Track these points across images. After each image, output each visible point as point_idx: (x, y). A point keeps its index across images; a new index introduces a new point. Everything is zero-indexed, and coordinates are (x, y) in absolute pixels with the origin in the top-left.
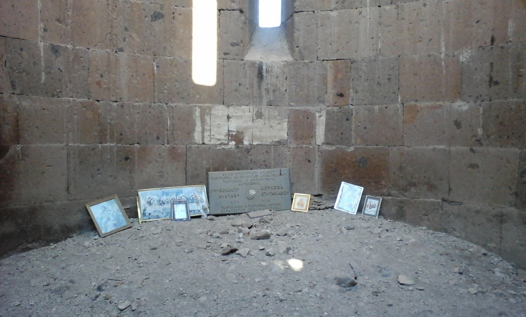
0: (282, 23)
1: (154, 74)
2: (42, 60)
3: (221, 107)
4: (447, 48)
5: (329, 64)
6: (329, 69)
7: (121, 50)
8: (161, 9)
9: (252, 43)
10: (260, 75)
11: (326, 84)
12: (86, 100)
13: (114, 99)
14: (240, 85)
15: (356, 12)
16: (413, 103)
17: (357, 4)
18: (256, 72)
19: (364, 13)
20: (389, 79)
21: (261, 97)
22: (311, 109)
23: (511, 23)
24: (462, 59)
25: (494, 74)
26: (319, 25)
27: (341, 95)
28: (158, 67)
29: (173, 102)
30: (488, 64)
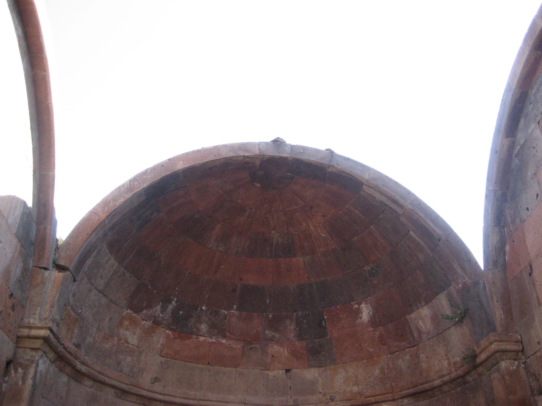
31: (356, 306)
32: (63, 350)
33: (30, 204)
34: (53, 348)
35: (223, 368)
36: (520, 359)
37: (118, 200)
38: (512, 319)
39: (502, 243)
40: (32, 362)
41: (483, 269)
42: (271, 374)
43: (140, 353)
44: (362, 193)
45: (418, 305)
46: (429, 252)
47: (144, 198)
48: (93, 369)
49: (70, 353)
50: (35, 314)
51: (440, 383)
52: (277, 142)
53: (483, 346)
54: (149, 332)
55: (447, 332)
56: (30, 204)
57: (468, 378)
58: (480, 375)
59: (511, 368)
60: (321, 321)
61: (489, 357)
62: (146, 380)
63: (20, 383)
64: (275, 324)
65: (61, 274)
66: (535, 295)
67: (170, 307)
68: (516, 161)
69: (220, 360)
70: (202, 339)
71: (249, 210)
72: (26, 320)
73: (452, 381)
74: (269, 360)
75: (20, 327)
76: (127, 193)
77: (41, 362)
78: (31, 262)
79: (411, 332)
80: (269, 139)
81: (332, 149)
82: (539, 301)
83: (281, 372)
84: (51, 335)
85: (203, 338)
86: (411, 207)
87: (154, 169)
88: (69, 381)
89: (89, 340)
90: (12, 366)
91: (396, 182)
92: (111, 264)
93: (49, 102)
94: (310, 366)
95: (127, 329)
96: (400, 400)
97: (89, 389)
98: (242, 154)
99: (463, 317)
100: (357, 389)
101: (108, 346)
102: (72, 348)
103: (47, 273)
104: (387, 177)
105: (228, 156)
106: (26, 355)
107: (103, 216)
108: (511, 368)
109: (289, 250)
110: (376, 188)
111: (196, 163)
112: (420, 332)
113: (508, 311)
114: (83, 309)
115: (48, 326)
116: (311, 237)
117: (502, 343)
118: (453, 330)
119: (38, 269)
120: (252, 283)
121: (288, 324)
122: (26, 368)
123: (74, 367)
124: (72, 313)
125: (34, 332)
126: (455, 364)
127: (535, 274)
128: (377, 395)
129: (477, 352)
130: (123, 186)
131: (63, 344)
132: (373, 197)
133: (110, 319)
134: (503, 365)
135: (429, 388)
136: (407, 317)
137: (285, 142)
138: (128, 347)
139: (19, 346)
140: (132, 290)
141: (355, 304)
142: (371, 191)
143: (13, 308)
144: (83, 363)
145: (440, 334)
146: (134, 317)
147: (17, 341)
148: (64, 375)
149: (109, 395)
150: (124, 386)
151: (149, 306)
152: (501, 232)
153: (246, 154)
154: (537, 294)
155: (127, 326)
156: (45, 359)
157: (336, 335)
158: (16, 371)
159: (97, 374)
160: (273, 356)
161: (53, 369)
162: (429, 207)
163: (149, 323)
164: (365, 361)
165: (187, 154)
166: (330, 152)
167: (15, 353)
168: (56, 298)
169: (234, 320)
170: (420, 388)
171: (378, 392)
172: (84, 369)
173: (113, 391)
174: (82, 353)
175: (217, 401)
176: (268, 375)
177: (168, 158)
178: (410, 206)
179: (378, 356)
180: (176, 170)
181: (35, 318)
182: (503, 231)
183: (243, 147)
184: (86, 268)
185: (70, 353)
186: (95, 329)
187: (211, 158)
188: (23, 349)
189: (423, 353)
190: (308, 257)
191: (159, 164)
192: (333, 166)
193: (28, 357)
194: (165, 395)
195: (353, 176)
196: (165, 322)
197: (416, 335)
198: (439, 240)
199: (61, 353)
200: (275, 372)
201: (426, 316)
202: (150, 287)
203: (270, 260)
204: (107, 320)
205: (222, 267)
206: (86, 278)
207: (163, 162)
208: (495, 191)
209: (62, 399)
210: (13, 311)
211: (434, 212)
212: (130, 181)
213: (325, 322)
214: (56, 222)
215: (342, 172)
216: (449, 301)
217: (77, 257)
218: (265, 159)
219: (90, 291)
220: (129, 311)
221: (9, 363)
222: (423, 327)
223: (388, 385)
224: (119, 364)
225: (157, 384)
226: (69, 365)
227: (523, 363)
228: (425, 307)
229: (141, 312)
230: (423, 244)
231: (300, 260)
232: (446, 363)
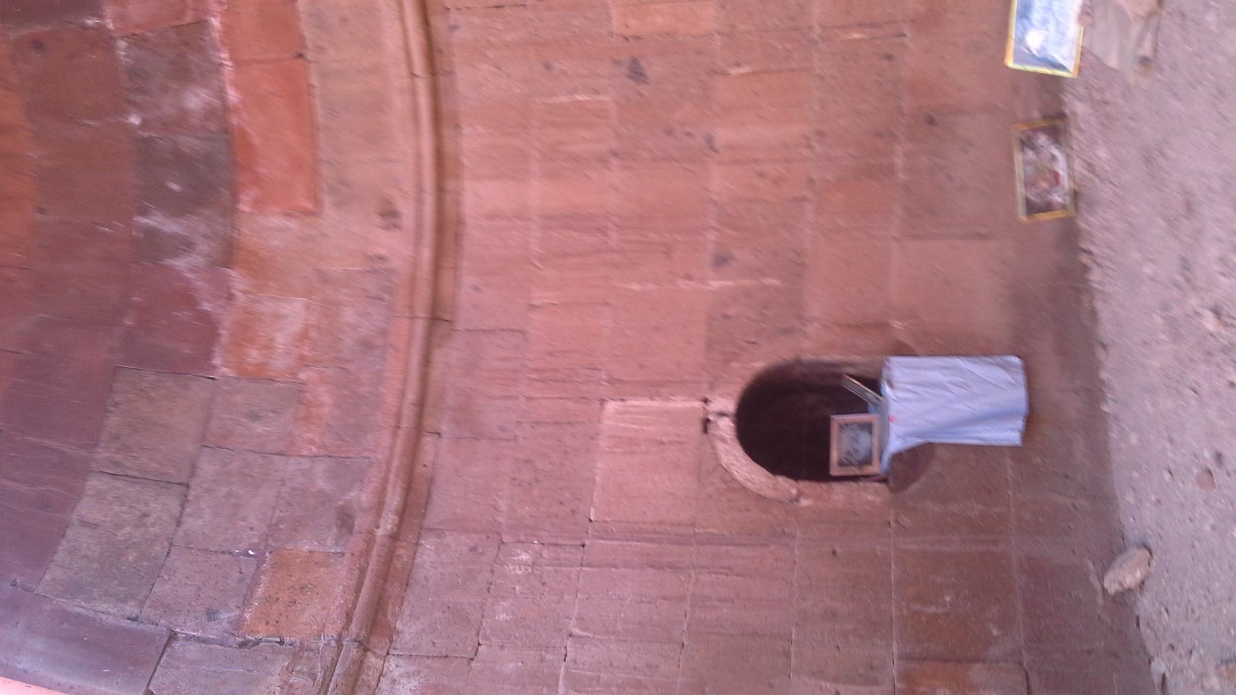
32: (354, 628)
48: (389, 462)
88: (431, 530)
92: (100, 506)
95: (268, 347)
97: (445, 441)
101: (325, 397)
114: (243, 545)
123: (394, 537)
124: (260, 591)
133: (255, 417)
140: (152, 378)
148: (418, 560)
149: (449, 356)
151: (187, 298)
159: (401, 433)
172: (394, 500)
184: (131, 608)
186: (292, 465)
204: (259, 428)
206: (157, 589)
209: (473, 549)
220: (217, 361)
224: (367, 345)
226: (391, 560)
229: (207, 314)
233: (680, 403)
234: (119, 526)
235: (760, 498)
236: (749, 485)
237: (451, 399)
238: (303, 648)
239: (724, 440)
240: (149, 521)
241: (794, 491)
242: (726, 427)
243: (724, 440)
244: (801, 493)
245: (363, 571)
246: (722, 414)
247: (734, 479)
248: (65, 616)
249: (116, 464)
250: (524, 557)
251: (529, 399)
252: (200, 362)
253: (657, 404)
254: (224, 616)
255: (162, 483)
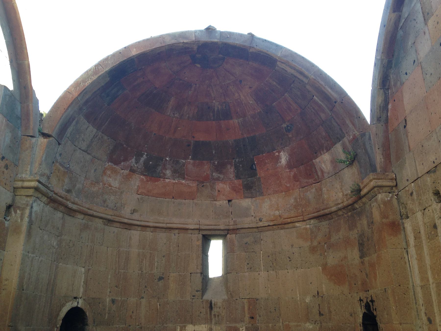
0: (223, 275)
1: (158, 309)
2: (107, 307)
3: (191, 326)
4: (300, 295)
5: (245, 301)
6: (245, 303)
7: (143, 298)
8: (163, 275)
9: (207, 288)
10: (211, 307)
11: (244, 312)
12: (124, 326)
13: (137, 324)
14: (201, 313)
15: (257, 274)
16: (287, 323)
17: (257, 269)
18: (209, 305)
19: (261, 275)
20: (275, 310)
21: (211, 319)
22: (238, 325)
23: (324, 286)
24: (307, 301)
25: (321, 310)
26: (240, 280)
27: (252, 318)
28: (160, 305)
29: (167, 324)
30: (318, 305)
31: (277, 154)
32: (54, 195)
33: (11, 87)
34: (44, 194)
35: (184, 201)
36: (394, 192)
37: (86, 82)
38: (390, 162)
39: (386, 102)
40: (27, 205)
41: (369, 122)
42: (218, 203)
43: (122, 193)
44: (277, 67)
45: (322, 152)
46: (329, 112)
47: (108, 79)
48: (82, 206)
49: (60, 197)
50: (26, 171)
51: (336, 209)
52: (210, 30)
53: (365, 183)
54: (127, 178)
55: (341, 172)
56: (11, 87)
57: (356, 206)
58: (364, 204)
59: (386, 199)
60: (252, 165)
61: (369, 191)
62: (126, 212)
63: (19, 221)
64: (220, 168)
65: (45, 140)
66: (407, 144)
67: (142, 160)
68: (401, 33)
69: (181, 195)
70: (167, 180)
71: (194, 85)
72: (19, 176)
73: (345, 208)
74: (216, 193)
75: (15, 181)
76: (93, 75)
77: (35, 205)
78: (20, 132)
79: (316, 171)
80: (203, 27)
81: (253, 33)
82: (409, 148)
83: (225, 202)
84: (40, 185)
85: (168, 180)
86: (314, 77)
87: (113, 55)
88: (63, 216)
89: (79, 186)
90: (12, 209)
91: (303, 58)
92: (90, 131)
93: (13, 2)
94: (246, 197)
95: (110, 177)
96: (308, 221)
98: (182, 41)
99: (352, 160)
100: (278, 213)
101: (95, 189)
102: (63, 193)
103: (34, 140)
104: (296, 54)
105: (171, 43)
106: (21, 201)
107: (76, 95)
108: (386, 199)
109: (226, 114)
110: (286, 63)
111: (145, 50)
112: (322, 172)
113: (387, 156)
115: (36, 179)
116: (242, 104)
117: (380, 180)
118: (346, 170)
119: (26, 137)
120: (201, 139)
121: (229, 168)
122: (23, 209)
123: (66, 207)
124: (61, 168)
125: (26, 184)
126: (346, 195)
127: (408, 127)
128: (292, 218)
129: (361, 188)
130: (90, 70)
131: (53, 191)
132: (286, 71)
133: (95, 170)
134: (380, 196)
135: (328, 213)
136: (314, 161)
137: (215, 29)
138: (111, 189)
139: (16, 194)
141: (276, 152)
142: (283, 66)
143: (6, 167)
144: (73, 203)
145: (336, 173)
146: (115, 168)
147: (14, 191)
148: (59, 212)
149: (99, 223)
150: (109, 217)
151: (125, 160)
152: (385, 94)
153: (185, 41)
154: (409, 143)
155: (109, 174)
156: (39, 202)
157: (263, 175)
158: (16, 212)
159: (87, 210)
160: (219, 191)
161: (48, 209)
162: (329, 76)
163: (126, 172)
164: (283, 193)
165: (139, 42)
166: (251, 36)
167: (13, 200)
168: (44, 158)
169: (190, 167)
170: (322, 212)
171: (292, 215)
172: (75, 207)
173: (101, 220)
174: (73, 196)
175: (180, 224)
176: (215, 204)
177: (124, 46)
178: (312, 76)
179: (293, 190)
180: (131, 56)
181: (27, 174)
182: (387, 92)
183: (183, 35)
184: (68, 135)
185: (60, 197)
186: (83, 179)
187: (158, 45)
188: (19, 196)
189: (324, 187)
190: (241, 119)
191: (117, 52)
192: (253, 48)
193: (24, 202)
194: (141, 221)
195: (269, 55)
196: (139, 170)
197: (320, 174)
198: (335, 102)
199: (52, 198)
200: (221, 202)
201: (327, 160)
202: (125, 146)
203: (214, 122)
204: (93, 171)
205: (179, 128)
207: (120, 50)
208: (382, 60)
209: (58, 229)
210: (7, 169)
211: (332, 80)
212: (96, 66)
213: (255, 166)
214: (37, 101)
215: (261, 51)
216: (344, 149)
217: (58, 127)
218: (200, 44)
219: (74, 151)
221: (9, 207)
222: (325, 168)
223: (300, 211)
224: (105, 201)
225: (135, 214)
226: (62, 205)
227: (396, 195)
228: (326, 154)
230: (324, 106)
231: (235, 122)
232: (341, 195)
233: (82, 290)
234: (84, 135)
235: (58, 315)
236: (61, 312)
237: (90, 223)
238: (49, 179)
239: (72, 303)
240: (82, 142)
241: (58, 326)
242: (75, 304)
243: (72, 303)
244: (57, 328)
245: (63, 198)
246: (78, 303)
247: (63, 307)
248: (73, 120)
249: (97, 136)
250: (55, 243)
251: (87, 245)
252: (111, 160)
253: (82, 283)
254: (60, 158)
255: (89, 146)
